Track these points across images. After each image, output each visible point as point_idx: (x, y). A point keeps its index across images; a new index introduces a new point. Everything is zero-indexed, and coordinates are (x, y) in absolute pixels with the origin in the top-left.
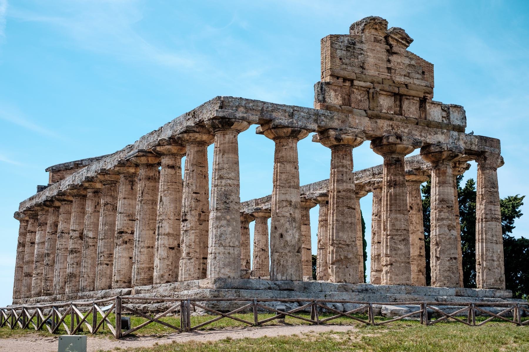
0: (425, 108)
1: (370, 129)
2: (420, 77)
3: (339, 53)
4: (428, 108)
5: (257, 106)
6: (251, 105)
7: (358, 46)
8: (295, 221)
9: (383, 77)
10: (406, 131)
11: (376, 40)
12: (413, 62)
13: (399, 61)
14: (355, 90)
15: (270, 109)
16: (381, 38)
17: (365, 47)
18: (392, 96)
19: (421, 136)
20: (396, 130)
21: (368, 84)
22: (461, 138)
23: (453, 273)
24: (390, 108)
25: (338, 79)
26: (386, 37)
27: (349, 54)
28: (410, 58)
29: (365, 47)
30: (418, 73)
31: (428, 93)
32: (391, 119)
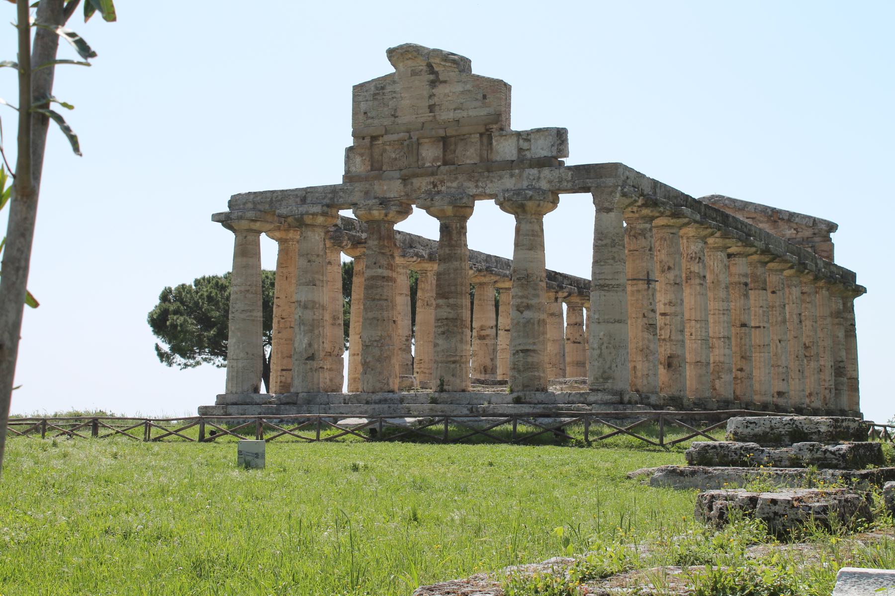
0: (491, 144)
1: (403, 194)
2: (478, 104)
3: (363, 106)
4: (494, 143)
5: (266, 198)
6: (259, 198)
7: (389, 89)
8: (303, 324)
9: (422, 120)
10: (455, 184)
11: (414, 73)
12: (469, 87)
13: (447, 91)
14: (387, 147)
15: (280, 197)
16: (421, 68)
17: (398, 88)
18: (439, 141)
19: (477, 186)
20: (440, 187)
21: (402, 135)
22: (542, 175)
23: (519, 371)
24: (435, 159)
25: (364, 139)
26: (430, 66)
27: (376, 103)
28: (464, 82)
29: (398, 88)
30: (477, 99)
31: (492, 123)
32: (433, 174)
